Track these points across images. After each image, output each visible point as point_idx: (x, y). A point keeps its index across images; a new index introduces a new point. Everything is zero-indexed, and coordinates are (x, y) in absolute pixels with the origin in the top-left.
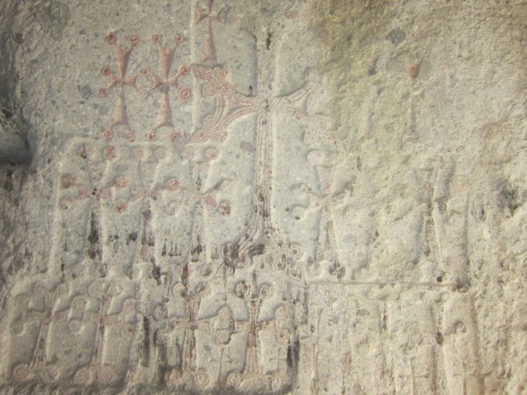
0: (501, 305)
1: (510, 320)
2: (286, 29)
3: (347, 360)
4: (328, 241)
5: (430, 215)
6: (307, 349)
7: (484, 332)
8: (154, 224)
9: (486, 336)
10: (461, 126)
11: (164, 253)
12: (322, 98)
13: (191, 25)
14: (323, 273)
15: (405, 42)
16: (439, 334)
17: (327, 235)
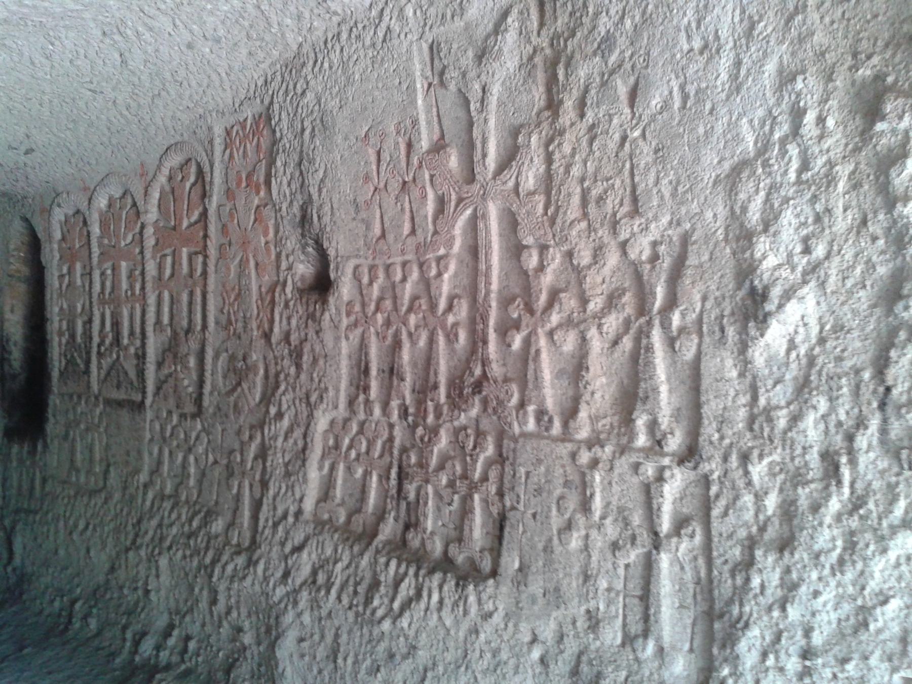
0: (748, 499)
1: (762, 529)
2: (497, 77)
3: (548, 549)
4: (536, 379)
5: (648, 337)
6: (512, 526)
7: (719, 542)
8: (406, 355)
9: (721, 550)
10: (695, 178)
11: (414, 391)
12: (534, 169)
13: (420, 102)
14: (531, 425)
15: (617, 52)
16: (656, 534)
17: (535, 370)
